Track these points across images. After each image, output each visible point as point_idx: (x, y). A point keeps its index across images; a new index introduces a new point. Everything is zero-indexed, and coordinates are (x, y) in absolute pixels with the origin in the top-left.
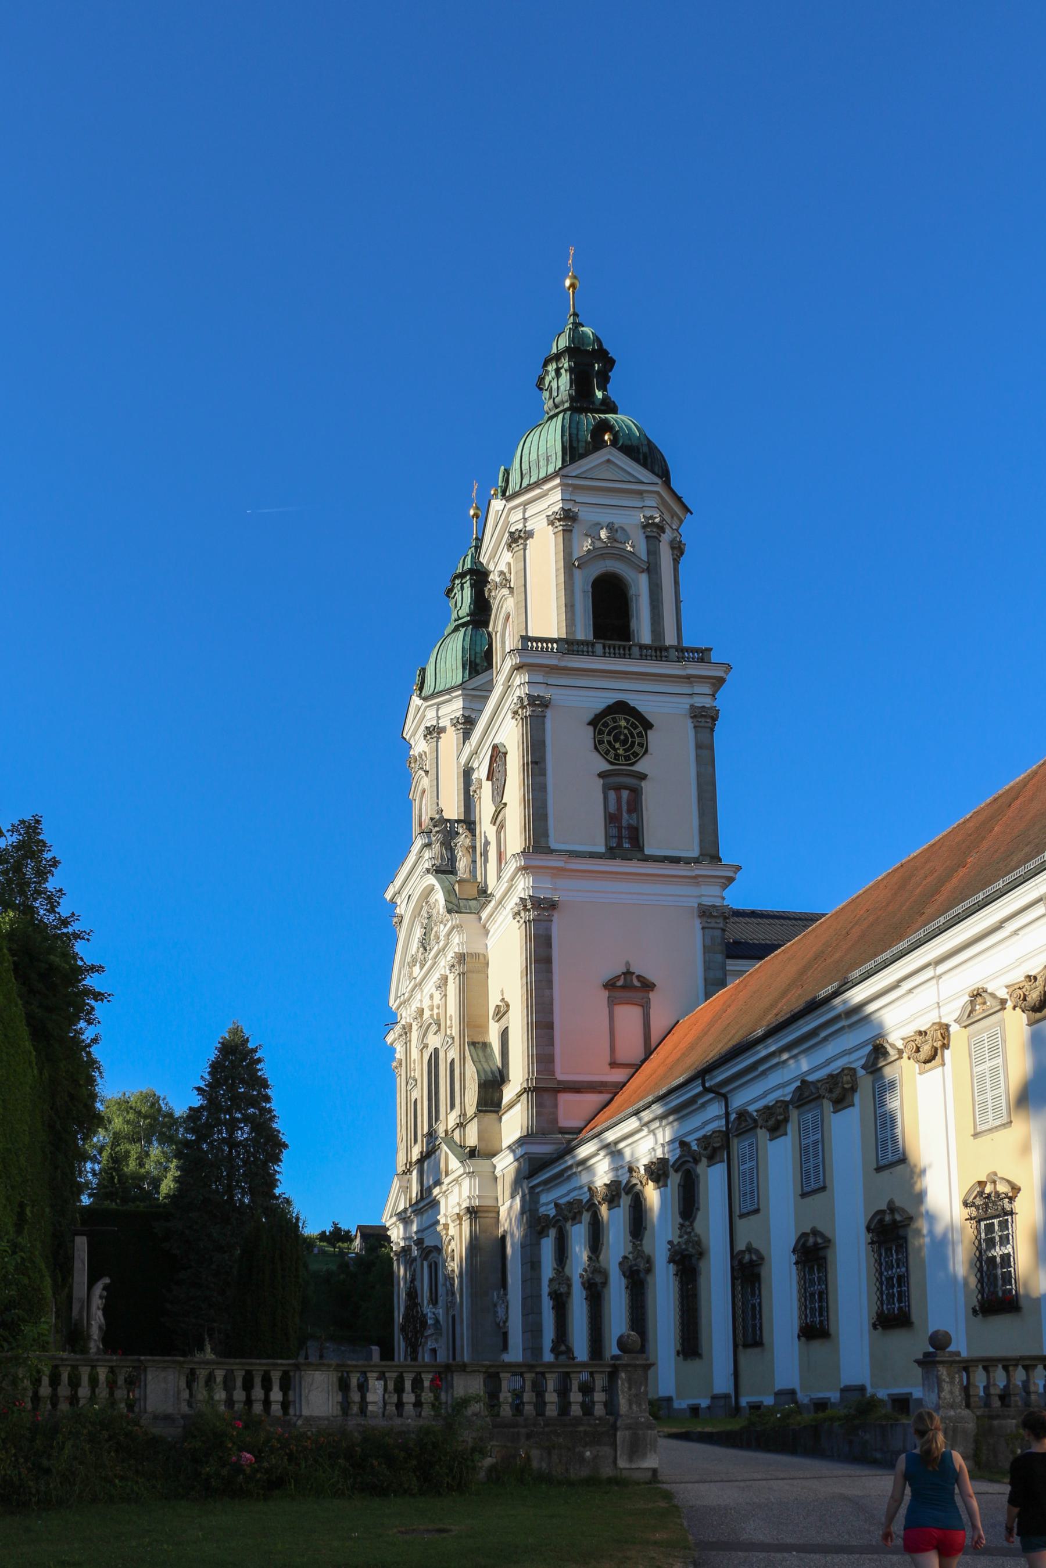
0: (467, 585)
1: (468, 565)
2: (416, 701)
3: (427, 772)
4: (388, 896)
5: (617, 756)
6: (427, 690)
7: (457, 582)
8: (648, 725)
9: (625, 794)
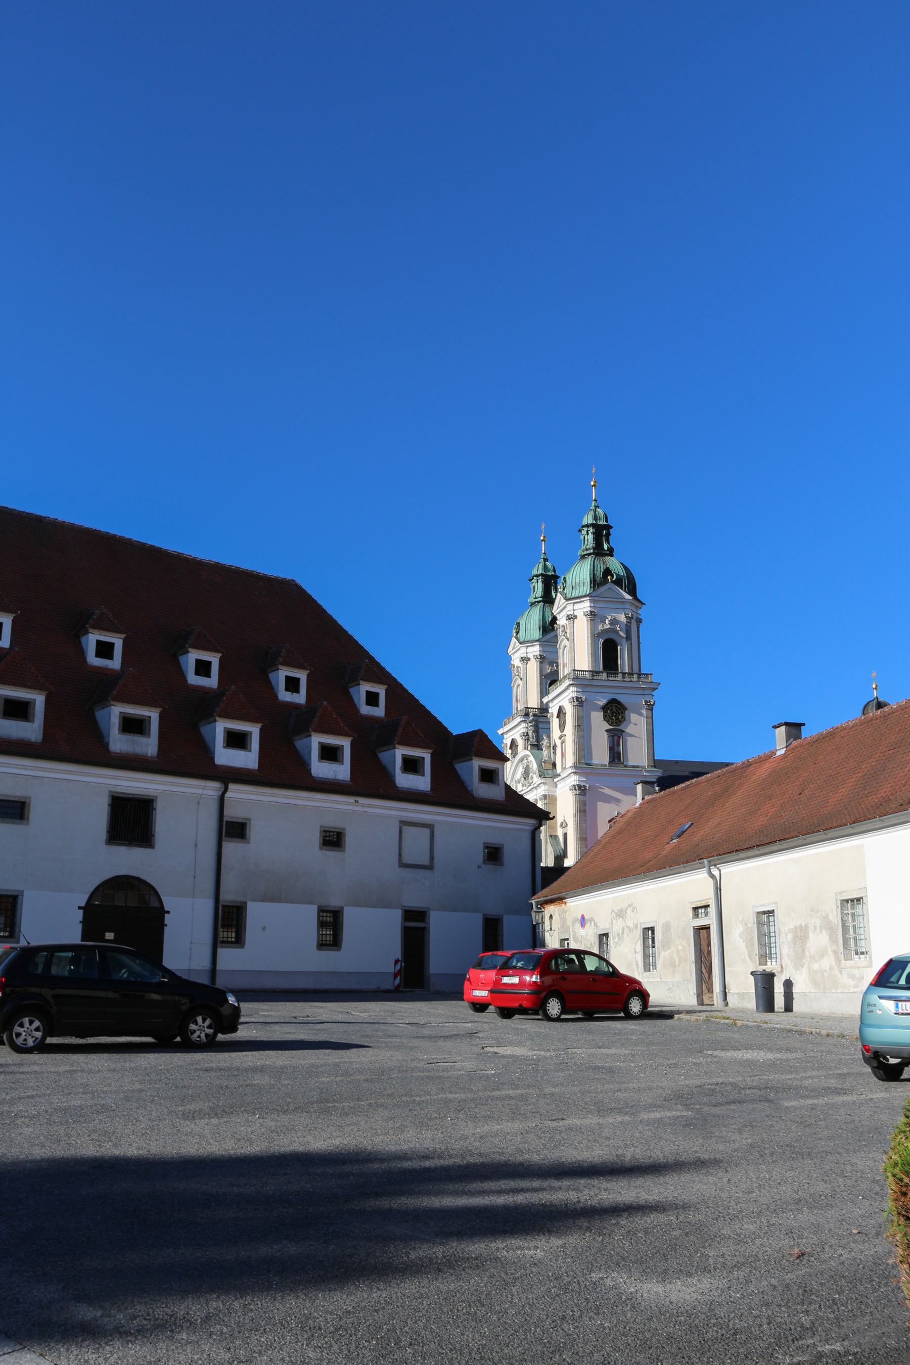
0: (540, 581)
1: (540, 572)
2: (514, 640)
3: (521, 679)
4: (500, 732)
5: (612, 723)
6: (521, 635)
7: (535, 578)
8: (625, 709)
9: (616, 738)
